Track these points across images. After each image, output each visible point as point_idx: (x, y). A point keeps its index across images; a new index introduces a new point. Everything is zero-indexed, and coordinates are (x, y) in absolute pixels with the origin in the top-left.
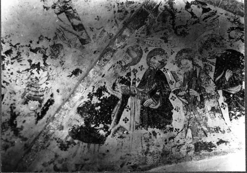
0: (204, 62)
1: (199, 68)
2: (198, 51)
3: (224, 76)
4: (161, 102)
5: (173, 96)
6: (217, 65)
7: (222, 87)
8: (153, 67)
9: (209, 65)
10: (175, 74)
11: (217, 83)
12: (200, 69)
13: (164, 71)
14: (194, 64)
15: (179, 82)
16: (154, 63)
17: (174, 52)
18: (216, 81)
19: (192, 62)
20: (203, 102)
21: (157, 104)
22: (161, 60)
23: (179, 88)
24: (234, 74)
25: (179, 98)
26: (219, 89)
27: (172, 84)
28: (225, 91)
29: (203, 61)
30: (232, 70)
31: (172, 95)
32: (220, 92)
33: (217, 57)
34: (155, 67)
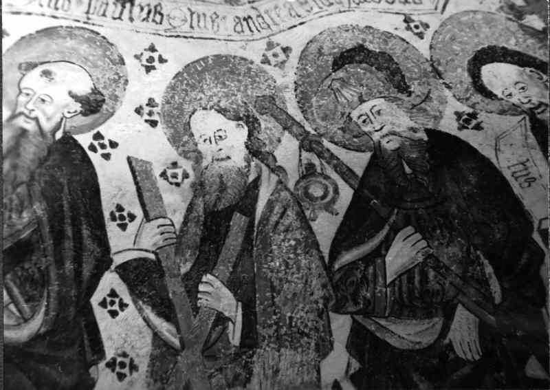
0: (305, 154)
1: (274, 178)
2: (292, 86)
3: (379, 253)
4: (46, 313)
5: (113, 294)
6: (363, 186)
7: (356, 303)
8: (36, 119)
9: (327, 177)
10: (148, 174)
11: (338, 276)
12: (280, 182)
13: (93, 148)
14: (254, 150)
15: (161, 221)
16: (43, 101)
17: (162, 60)
18: (337, 266)
19: (250, 135)
20: (251, 356)
21: (26, 321)
22: (84, 86)
23: (152, 256)
24: (428, 256)
25: (140, 310)
26: (338, 310)
27: (123, 227)
28: (364, 328)
29: (301, 147)
30: (426, 233)
31: (110, 281)
32: (341, 326)
33: (377, 151)
34: (49, 119)
